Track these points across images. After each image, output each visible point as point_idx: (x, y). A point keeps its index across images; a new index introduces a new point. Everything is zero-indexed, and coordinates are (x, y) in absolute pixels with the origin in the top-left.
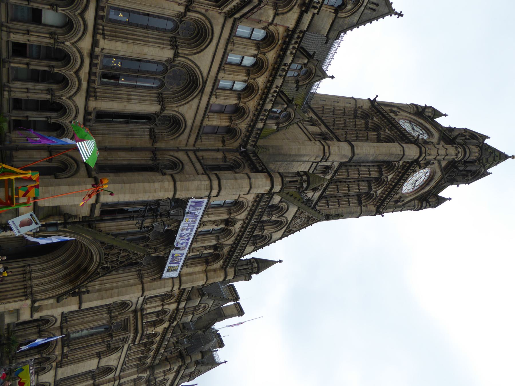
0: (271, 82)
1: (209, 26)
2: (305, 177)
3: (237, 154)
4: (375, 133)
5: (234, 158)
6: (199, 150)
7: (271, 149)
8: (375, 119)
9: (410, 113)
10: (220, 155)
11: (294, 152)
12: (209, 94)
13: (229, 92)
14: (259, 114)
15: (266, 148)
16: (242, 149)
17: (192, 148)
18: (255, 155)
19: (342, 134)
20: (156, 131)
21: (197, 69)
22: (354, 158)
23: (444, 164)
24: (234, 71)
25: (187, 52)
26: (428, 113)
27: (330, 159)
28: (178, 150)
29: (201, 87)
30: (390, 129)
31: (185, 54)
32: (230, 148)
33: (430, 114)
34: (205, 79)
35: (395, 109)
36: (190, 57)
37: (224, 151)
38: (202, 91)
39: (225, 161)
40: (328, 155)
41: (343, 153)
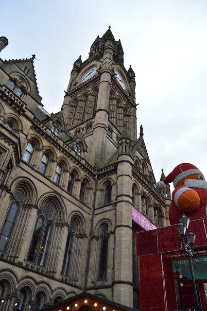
0: (60, 148)
1: (21, 179)
2: (124, 140)
3: (99, 182)
4: (89, 97)
5: (102, 184)
6: (94, 206)
7: (97, 160)
8: (80, 95)
10: (99, 193)
11: (100, 145)
13: (61, 177)
15: (96, 163)
17: (91, 211)
18: (101, 170)
20: (78, 233)
23: (114, 62)
24: (50, 170)
26: (79, 65)
27: (106, 125)
28: (92, 220)
30: (88, 87)
33: (79, 65)
35: (74, 83)
39: (103, 190)
41: (104, 116)
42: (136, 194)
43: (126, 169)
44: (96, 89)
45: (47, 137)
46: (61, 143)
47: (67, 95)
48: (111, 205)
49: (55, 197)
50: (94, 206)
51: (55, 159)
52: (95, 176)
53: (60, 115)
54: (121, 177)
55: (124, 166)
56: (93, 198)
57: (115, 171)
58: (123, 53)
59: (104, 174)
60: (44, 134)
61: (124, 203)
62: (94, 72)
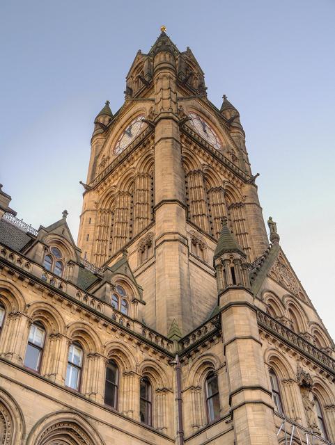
2: (225, 256)
3: (185, 369)
4: (138, 181)
5: (192, 373)
6: (181, 432)
7: (172, 318)
8: (115, 184)
9: (106, 142)
11: (176, 283)
12: (89, 405)
13: (85, 372)
14: (122, 328)
15: (172, 325)
16: (176, 360)
18: (187, 338)
19: (139, 224)
21: (48, 421)
22: (181, 201)
23: (180, 95)
25: (20, 434)
27: (184, 233)
29: (77, 417)
31: (23, 438)
32: (174, 380)
33: (107, 119)
34: (66, 409)
35: (100, 161)
36: (28, 430)
37: (181, 392)
38: (85, 416)
39: (199, 388)
40: (177, 236)
41: (174, 215)
42: (284, 381)
43: (241, 322)
44: (150, 161)
45: (33, 281)
46: (70, 290)
47: (88, 189)
48: (223, 419)
49: (74, 424)
50: (181, 432)
51: (61, 330)
52: (172, 357)
53: (59, 230)
54: (233, 345)
55: (235, 316)
56: (176, 413)
57: (218, 332)
58: (201, 74)
59: (195, 348)
60: (23, 276)
61: (249, 408)
62: (138, 128)
